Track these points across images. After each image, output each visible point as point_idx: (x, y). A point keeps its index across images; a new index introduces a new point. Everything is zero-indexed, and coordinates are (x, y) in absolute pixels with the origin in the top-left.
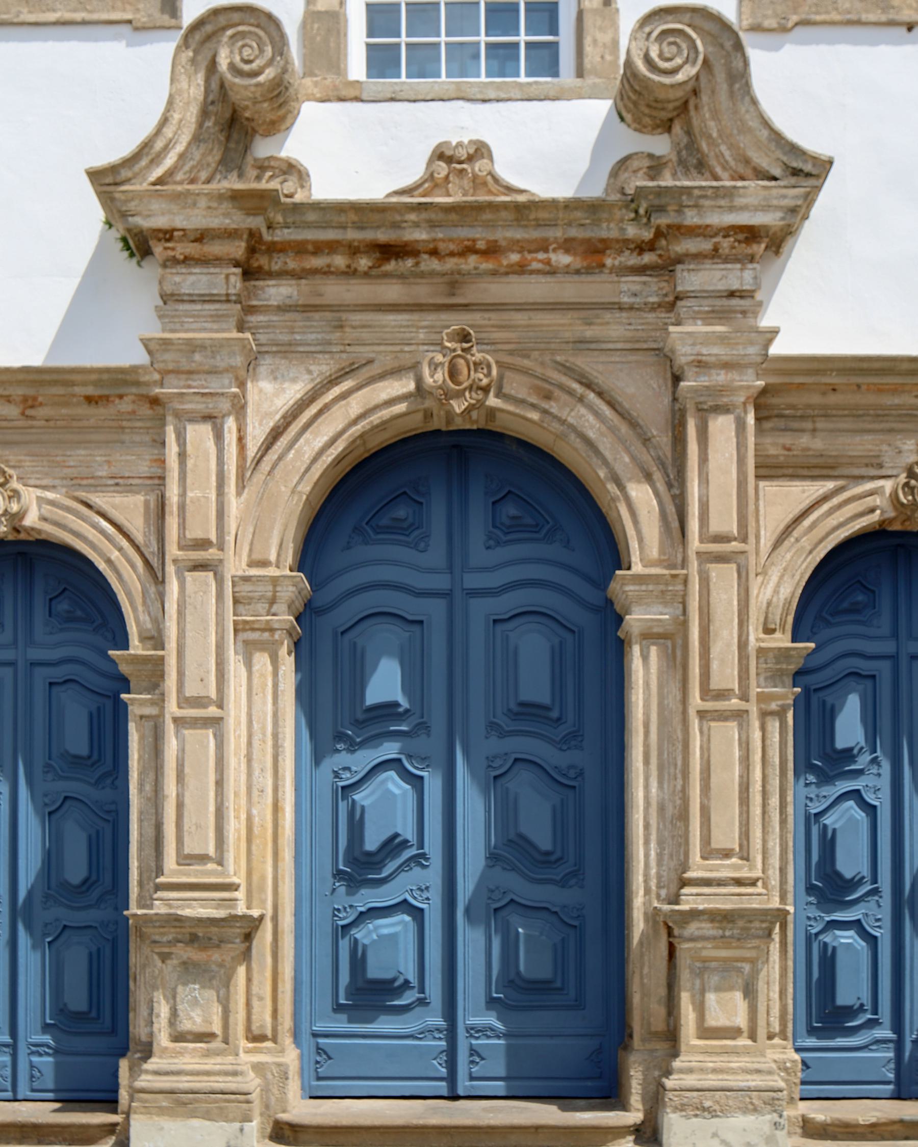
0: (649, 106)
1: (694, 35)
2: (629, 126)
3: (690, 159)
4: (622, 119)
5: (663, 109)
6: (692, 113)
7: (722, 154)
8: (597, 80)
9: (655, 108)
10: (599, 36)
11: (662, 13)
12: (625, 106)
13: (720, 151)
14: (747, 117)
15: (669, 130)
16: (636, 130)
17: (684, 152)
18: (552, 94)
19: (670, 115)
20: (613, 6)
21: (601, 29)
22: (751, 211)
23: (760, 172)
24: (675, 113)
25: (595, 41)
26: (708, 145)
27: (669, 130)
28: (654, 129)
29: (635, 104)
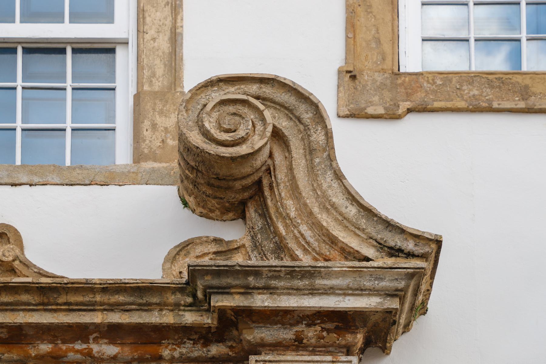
0: (209, 185)
1: (262, 107)
2: (193, 211)
3: (265, 243)
4: (185, 204)
5: (229, 188)
6: (267, 193)
7: (302, 235)
8: (156, 165)
9: (219, 187)
10: (159, 120)
11: (221, 84)
12: (186, 189)
13: (300, 232)
14: (330, 192)
15: (243, 216)
16: (201, 215)
17: (259, 236)
18: (99, 179)
19: (240, 197)
20: (179, 89)
21: (161, 113)
22: (339, 295)
23: (349, 253)
24: (246, 195)
25: (154, 126)
26: (286, 226)
27: (243, 216)
28: (223, 213)
29: (195, 184)
